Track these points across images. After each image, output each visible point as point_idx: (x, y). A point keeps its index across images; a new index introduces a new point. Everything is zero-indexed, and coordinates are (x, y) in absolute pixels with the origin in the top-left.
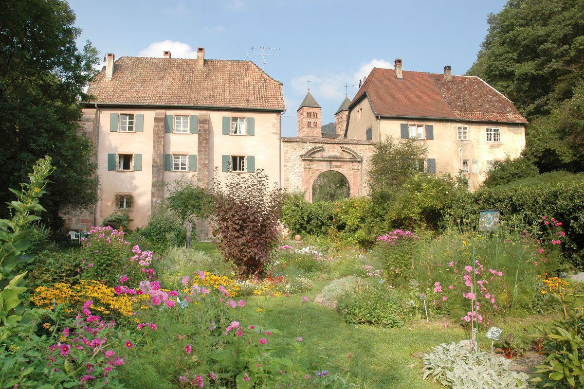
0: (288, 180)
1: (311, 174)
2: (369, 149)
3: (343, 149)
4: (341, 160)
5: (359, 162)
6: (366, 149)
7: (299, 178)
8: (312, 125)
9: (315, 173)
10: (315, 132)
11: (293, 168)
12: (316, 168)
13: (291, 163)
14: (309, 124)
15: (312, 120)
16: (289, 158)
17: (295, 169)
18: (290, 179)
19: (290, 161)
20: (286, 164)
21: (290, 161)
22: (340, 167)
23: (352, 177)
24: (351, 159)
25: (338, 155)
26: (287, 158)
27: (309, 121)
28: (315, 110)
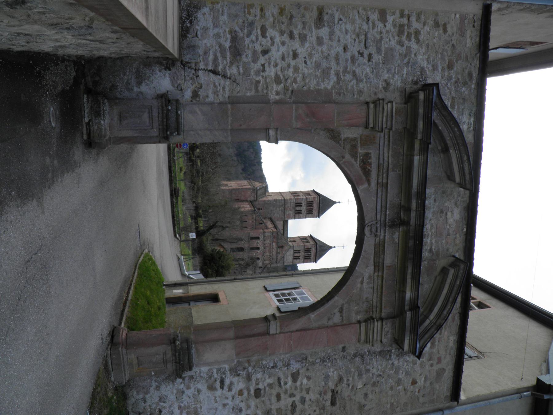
0: (319, 21)
1: (348, 133)
2: (440, 373)
3: (452, 271)
4: (409, 271)
5: (398, 342)
6: (439, 360)
7: (334, 78)
8: (298, 208)
9: (354, 155)
10: (290, 212)
11: (372, 49)
12: (374, 161)
13: (393, 43)
14: (299, 204)
15: (304, 208)
16: (417, 33)
17: (370, 57)
18: (324, 32)
19: (404, 38)
20: (390, 19)
21: (404, 38)
22: (378, 266)
23: (337, 319)
24: (414, 307)
25: (426, 254)
26: (415, 25)
27: (303, 205)
28: (315, 212)
